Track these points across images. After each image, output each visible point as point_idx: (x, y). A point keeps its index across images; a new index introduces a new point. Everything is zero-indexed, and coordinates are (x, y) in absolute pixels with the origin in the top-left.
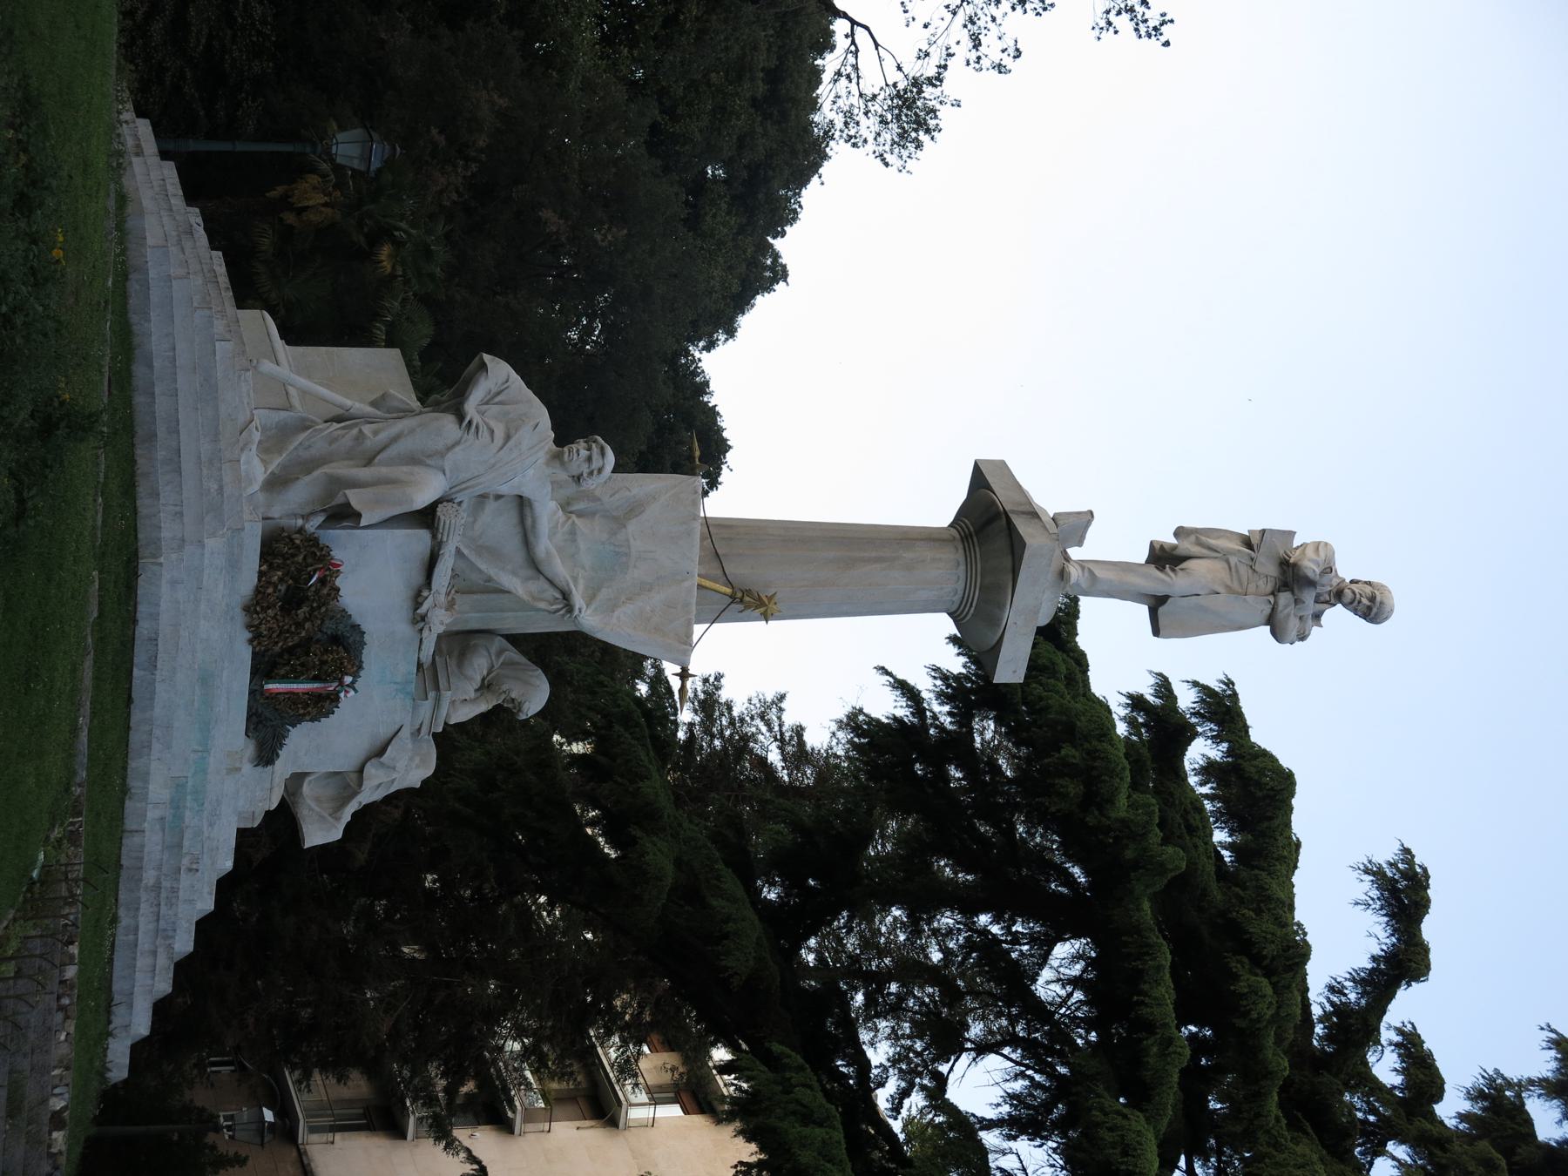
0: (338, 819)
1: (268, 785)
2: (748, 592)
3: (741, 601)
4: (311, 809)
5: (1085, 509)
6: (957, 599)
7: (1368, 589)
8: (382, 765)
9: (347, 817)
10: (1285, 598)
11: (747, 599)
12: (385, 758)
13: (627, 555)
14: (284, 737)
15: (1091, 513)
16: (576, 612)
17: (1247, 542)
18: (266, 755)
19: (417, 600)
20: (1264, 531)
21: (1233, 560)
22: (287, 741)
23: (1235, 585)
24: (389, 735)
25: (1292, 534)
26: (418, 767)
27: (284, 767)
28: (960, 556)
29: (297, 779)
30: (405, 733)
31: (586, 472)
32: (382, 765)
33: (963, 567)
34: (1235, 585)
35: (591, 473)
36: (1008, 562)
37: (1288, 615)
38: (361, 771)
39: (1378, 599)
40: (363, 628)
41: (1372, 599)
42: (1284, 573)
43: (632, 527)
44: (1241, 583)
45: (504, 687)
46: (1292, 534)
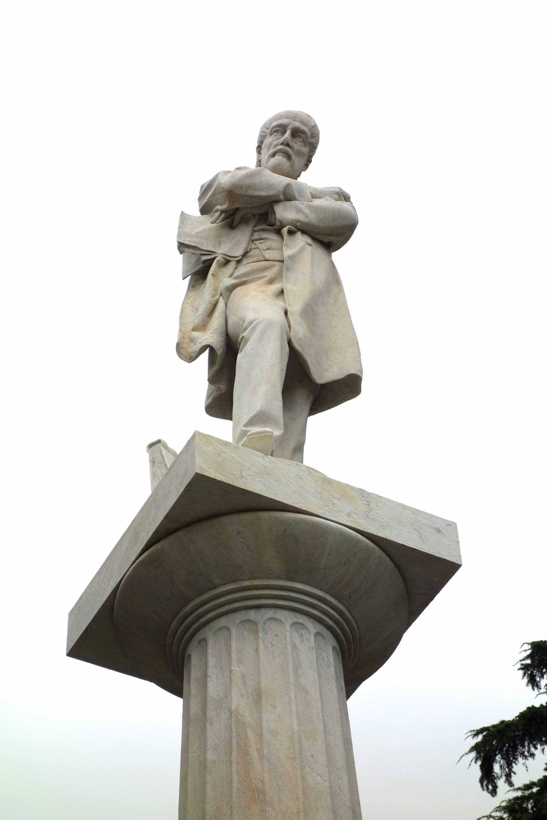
5: (146, 457)
6: (312, 627)
7: (268, 140)
10: (285, 213)
15: (151, 446)
17: (200, 274)
20: (182, 247)
21: (228, 282)
23: (270, 274)
25: (183, 216)
33: (252, 614)
34: (270, 274)
36: (233, 523)
37: (310, 207)
39: (284, 121)
41: (281, 129)
42: (244, 221)
44: (265, 269)
46: (183, 216)
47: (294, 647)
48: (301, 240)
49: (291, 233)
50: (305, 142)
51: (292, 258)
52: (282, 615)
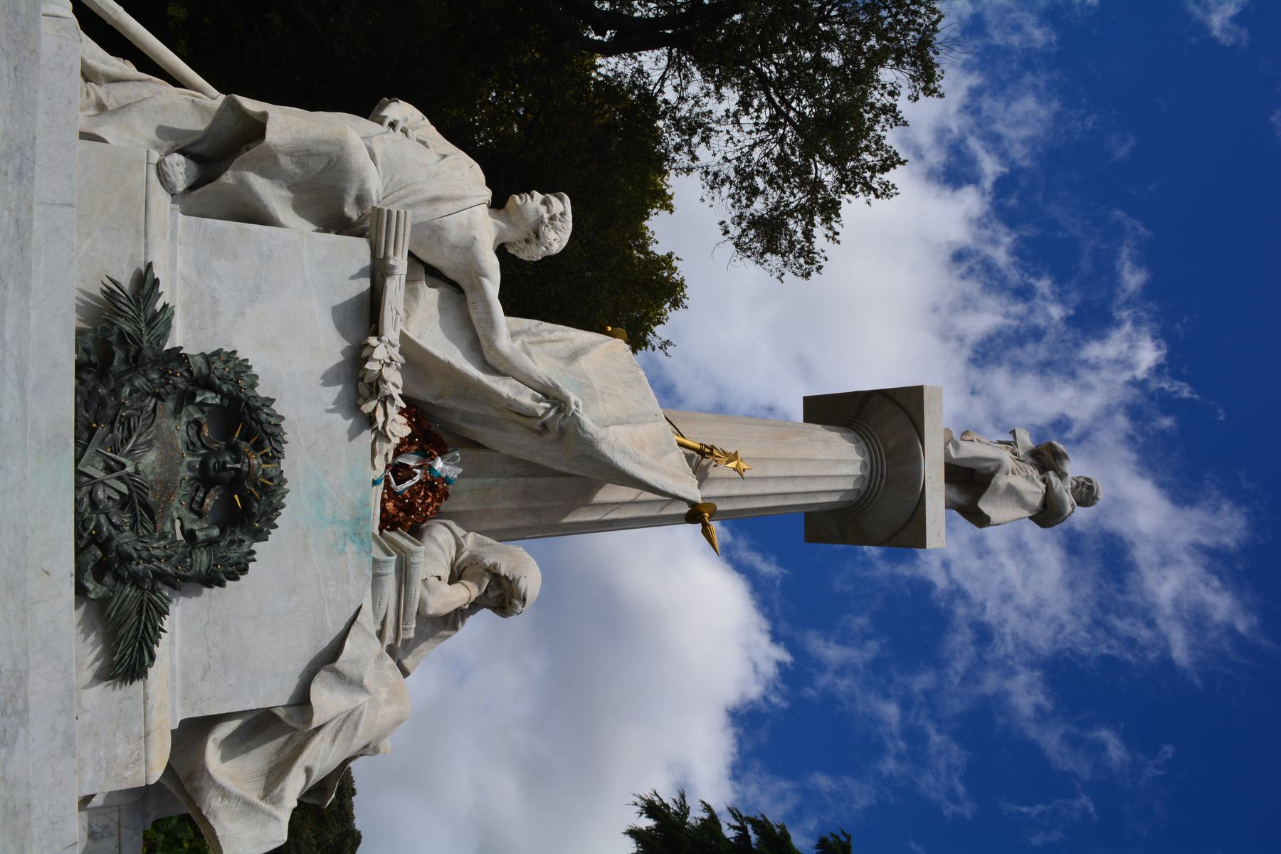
0: (277, 801)
1: (139, 728)
2: (712, 448)
3: (711, 454)
4: (225, 793)
6: (867, 474)
8: (339, 675)
9: (291, 802)
11: (716, 453)
12: (341, 663)
13: (591, 387)
14: (163, 613)
16: (574, 407)
18: (127, 657)
19: (357, 357)
22: (167, 623)
24: (341, 627)
26: (388, 702)
27: (168, 692)
28: (853, 434)
29: (192, 732)
30: (368, 621)
31: (546, 216)
32: (339, 675)
35: (552, 218)
38: (302, 700)
40: (277, 408)
42: (1039, 460)
43: (583, 362)
45: (489, 561)
47: (854, 462)
48: (1043, 486)
49: (1044, 481)
50: (1088, 495)
51: (1033, 480)
52: (867, 455)
